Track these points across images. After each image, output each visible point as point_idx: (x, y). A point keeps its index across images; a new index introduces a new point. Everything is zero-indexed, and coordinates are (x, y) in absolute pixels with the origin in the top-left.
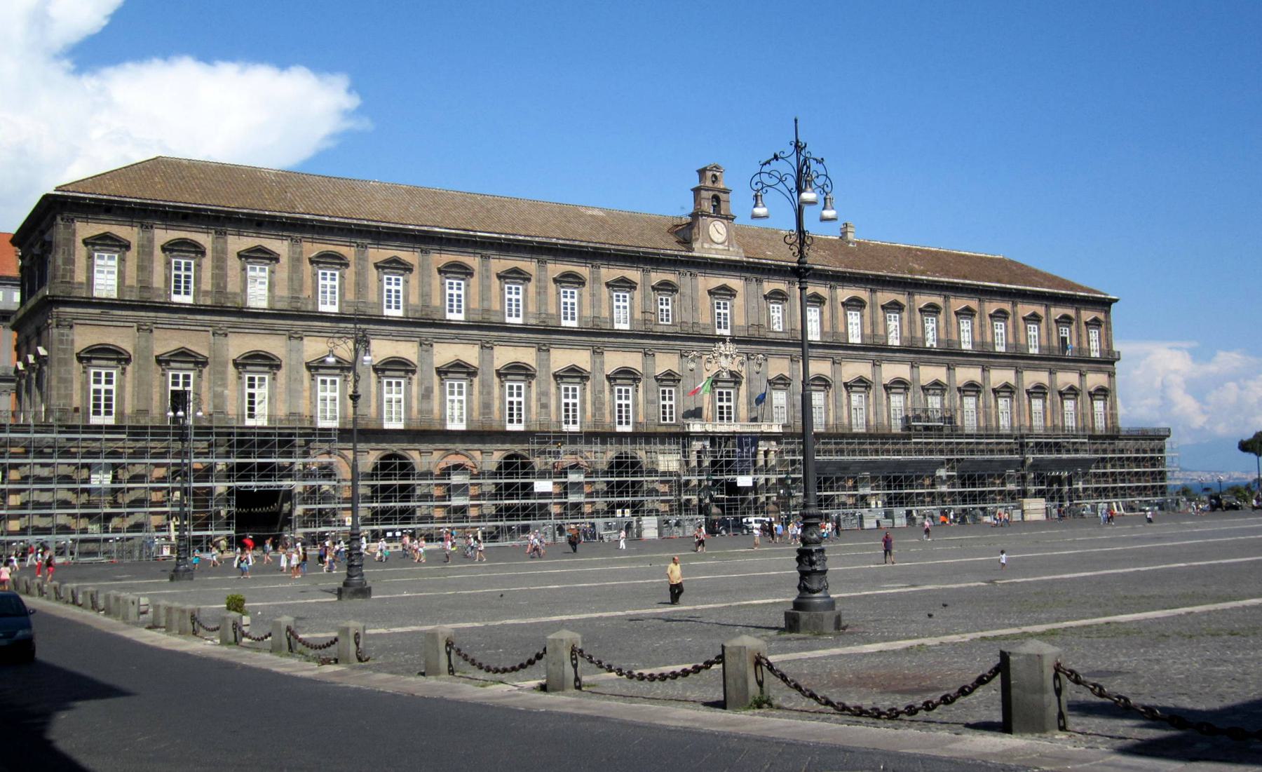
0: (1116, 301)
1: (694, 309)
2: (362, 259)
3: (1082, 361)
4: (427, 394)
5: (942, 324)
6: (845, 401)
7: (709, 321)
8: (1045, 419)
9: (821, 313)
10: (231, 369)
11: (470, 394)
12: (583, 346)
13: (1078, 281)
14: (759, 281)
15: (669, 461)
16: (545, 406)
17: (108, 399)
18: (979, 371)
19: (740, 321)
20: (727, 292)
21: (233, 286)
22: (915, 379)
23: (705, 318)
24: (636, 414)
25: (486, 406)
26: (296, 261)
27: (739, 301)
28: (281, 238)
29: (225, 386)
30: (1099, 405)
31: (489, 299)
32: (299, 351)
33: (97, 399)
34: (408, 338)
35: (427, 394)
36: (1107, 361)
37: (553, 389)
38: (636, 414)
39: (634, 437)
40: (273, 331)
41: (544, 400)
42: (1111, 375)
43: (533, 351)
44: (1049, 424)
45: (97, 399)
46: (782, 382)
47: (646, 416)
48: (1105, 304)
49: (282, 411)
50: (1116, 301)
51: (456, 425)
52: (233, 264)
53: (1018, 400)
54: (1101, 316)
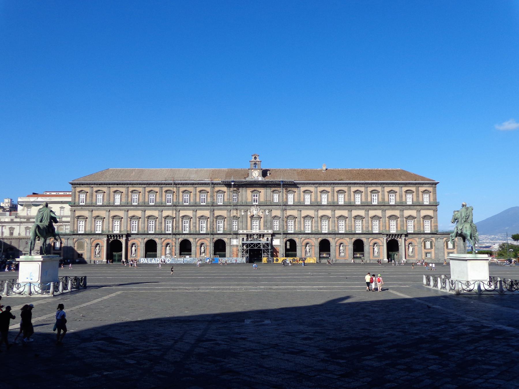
5: (346, 196)
7: (250, 200)
8: (397, 228)
9: (294, 196)
13: (429, 178)
15: (235, 242)
16: (195, 227)
18: (398, 211)
19: (262, 199)
21: (112, 201)
23: (249, 199)
36: (434, 205)
37: (198, 222)
39: (329, 234)
42: (436, 211)
44: (399, 229)
48: (434, 184)
51: (342, 231)
52: (112, 194)
54: (430, 189)
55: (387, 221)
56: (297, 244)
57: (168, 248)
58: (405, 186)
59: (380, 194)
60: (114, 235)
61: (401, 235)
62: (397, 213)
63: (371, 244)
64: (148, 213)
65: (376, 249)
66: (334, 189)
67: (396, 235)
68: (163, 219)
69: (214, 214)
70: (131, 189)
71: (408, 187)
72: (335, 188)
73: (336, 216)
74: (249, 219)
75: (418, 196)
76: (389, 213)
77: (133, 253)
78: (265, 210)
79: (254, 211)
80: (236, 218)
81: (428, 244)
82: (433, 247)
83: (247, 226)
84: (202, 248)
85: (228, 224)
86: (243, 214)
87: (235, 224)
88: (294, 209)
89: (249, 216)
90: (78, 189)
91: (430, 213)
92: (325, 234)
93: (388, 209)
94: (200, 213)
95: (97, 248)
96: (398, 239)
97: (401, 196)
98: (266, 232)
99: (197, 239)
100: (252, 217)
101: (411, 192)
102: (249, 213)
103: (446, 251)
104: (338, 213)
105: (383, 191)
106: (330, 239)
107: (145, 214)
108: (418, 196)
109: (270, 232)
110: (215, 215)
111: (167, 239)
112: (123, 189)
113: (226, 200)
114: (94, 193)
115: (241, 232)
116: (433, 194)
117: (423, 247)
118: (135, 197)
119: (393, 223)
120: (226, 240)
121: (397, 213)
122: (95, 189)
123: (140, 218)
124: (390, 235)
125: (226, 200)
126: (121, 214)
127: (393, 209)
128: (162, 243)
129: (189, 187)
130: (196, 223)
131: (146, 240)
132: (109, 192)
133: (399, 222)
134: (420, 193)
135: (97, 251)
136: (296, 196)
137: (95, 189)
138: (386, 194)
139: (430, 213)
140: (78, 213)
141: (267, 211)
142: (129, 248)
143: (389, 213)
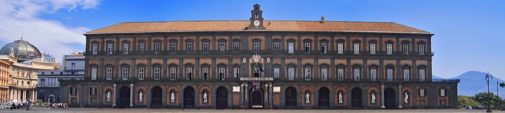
0: (433, 35)
1: (247, 46)
2: (150, 40)
3: (414, 56)
4: (165, 72)
5: (346, 45)
6: (302, 71)
10: (120, 67)
11: (177, 71)
12: (210, 58)
14: (272, 36)
15: (236, 89)
16: (197, 74)
17: (174, 75)
19: (263, 48)
20: (260, 41)
22: (333, 63)
23: (250, 48)
24: (226, 76)
25: (181, 74)
26: (135, 42)
27: (263, 43)
28: (130, 37)
29: (118, 71)
30: (422, 72)
31: (182, 48)
32: (135, 63)
33: (172, 75)
34: (161, 58)
35: (165, 72)
36: (429, 56)
37: (200, 70)
38: (226, 76)
40: (129, 59)
41: (197, 72)
43: (195, 60)
44: (395, 77)
45: (172, 75)
46: (277, 65)
47: (229, 76)
48: (429, 36)
49: (130, 76)
50: (433, 35)
53: (380, 70)
54: (426, 40)
55: (384, 70)
56: (297, 92)
57: (173, 94)
58: (402, 37)
59: (378, 44)
60: (122, 82)
61: (398, 83)
62: (394, 62)
63: (369, 91)
64: (154, 61)
65: (374, 97)
66: (333, 39)
67: (393, 83)
68: (168, 67)
69: (215, 62)
70: (138, 39)
71: (405, 38)
72: (335, 38)
73: (335, 64)
74: (250, 67)
75: (413, 47)
76: (386, 62)
77: (140, 99)
78: (265, 59)
79: (256, 59)
80: (236, 65)
81: (422, 92)
82: (427, 96)
83: (248, 73)
84: (205, 95)
85: (229, 72)
86: (244, 61)
87: (235, 70)
88: (294, 58)
89: (250, 65)
90: (91, 40)
91: (425, 62)
92: (325, 82)
93: (386, 59)
94: (202, 61)
95: (109, 94)
96: (395, 88)
97: (398, 47)
98: (267, 79)
99: (200, 86)
100: (253, 64)
101: (407, 42)
102: (251, 62)
103: (439, 98)
104: (337, 62)
105: (381, 42)
106: (329, 87)
107: (151, 63)
108: (413, 47)
109: (271, 79)
110: (217, 63)
111: (171, 86)
112: (131, 40)
113: (227, 49)
114: (105, 44)
115: (242, 79)
116: (428, 44)
117: (418, 96)
118: (142, 46)
119: (390, 71)
120: (227, 87)
121: (394, 62)
122: (106, 40)
123: (146, 66)
124: (388, 83)
125: (227, 49)
126: (129, 62)
127: (390, 59)
128: (166, 90)
129: (192, 36)
130: (198, 71)
131: (152, 87)
132: (119, 42)
133: (395, 71)
134: (416, 45)
135: (108, 97)
136: (297, 45)
137: (106, 40)
138: (384, 44)
139: (425, 62)
140: (90, 63)
141: (268, 59)
142: (136, 94)
143: (386, 62)
